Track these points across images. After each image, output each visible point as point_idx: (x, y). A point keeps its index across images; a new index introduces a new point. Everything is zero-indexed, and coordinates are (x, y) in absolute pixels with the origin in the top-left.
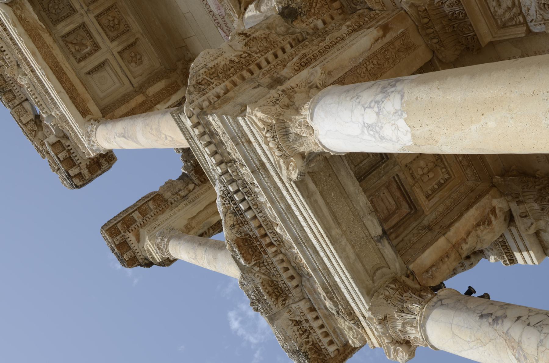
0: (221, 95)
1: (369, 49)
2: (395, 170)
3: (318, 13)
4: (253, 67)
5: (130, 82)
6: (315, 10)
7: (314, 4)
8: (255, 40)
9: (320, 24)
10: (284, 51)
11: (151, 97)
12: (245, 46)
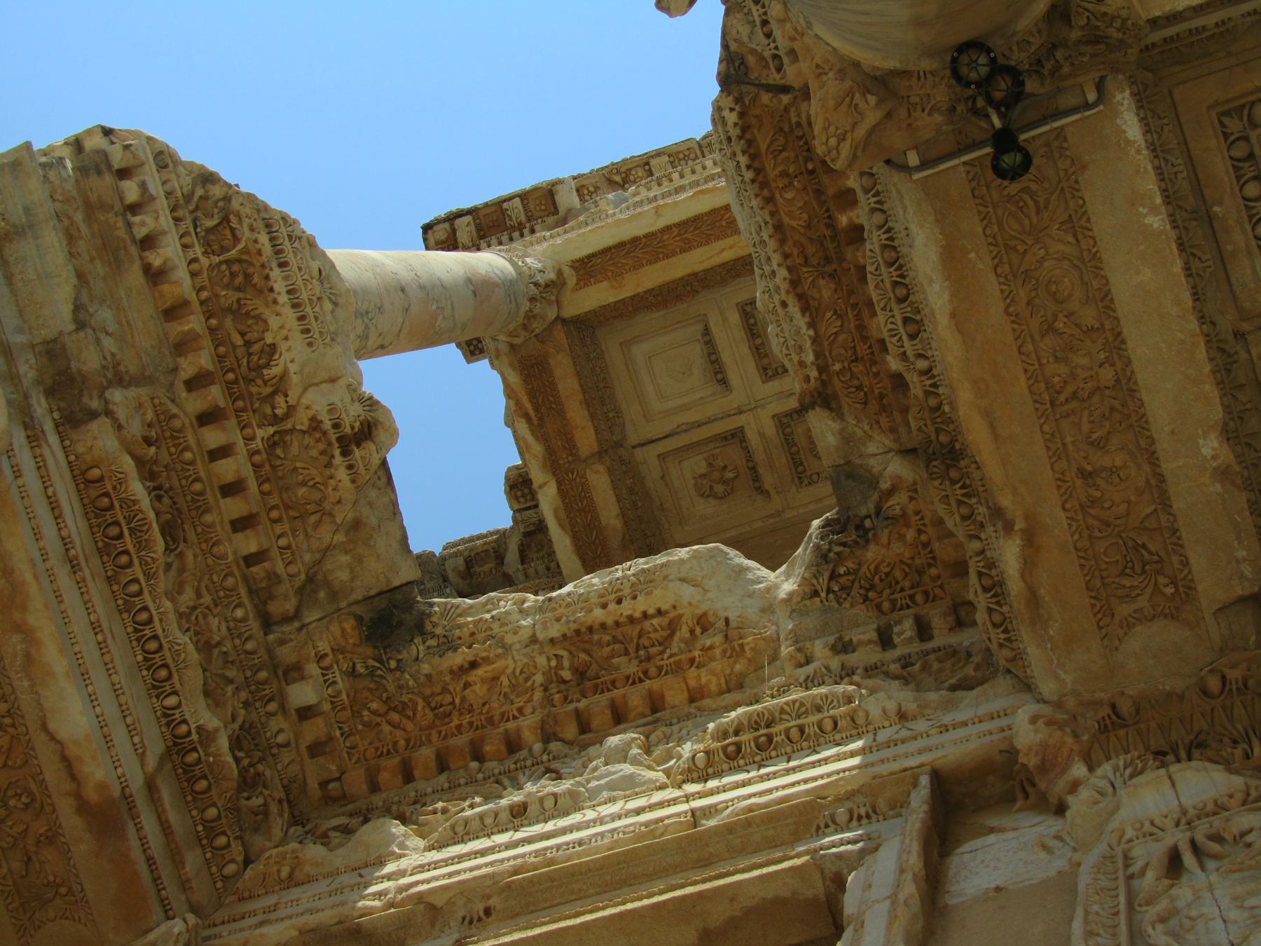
0: (147, 253)
1: (44, 727)
3: (356, 714)
4: (216, 394)
5: (652, 441)
6: (374, 713)
7: (395, 717)
8: (324, 459)
9: (303, 693)
10: (241, 524)
11: (583, 476)
12: (313, 419)
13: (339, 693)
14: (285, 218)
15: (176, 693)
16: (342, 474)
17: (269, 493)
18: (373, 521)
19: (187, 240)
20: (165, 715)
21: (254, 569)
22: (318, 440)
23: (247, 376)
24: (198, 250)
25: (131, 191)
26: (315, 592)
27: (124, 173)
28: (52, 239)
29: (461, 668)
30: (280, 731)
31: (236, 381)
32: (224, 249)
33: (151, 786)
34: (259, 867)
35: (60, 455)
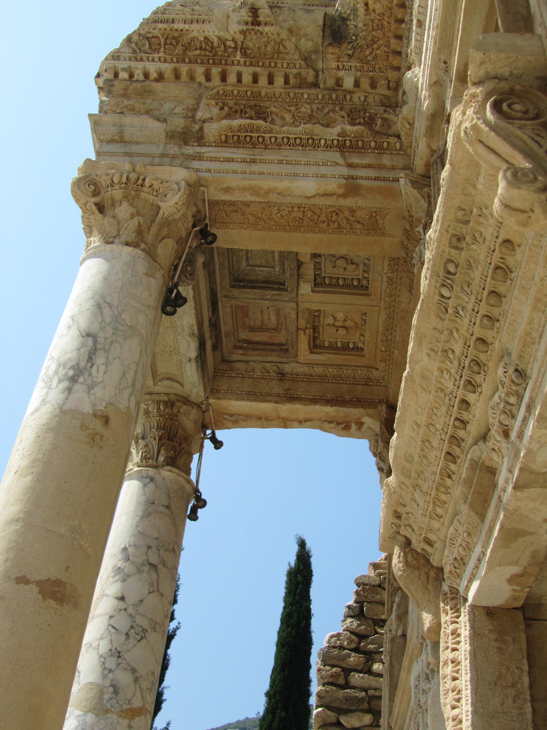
0: (151, 78)
1: (309, 198)
2: (288, 305)
3: (367, 62)
4: (215, 71)
6: (370, 54)
7: (375, 46)
8: (258, 34)
10: (271, 81)
12: (240, 33)
13: (356, 66)
14: (154, 13)
15: (320, 139)
16: (267, 29)
17: (264, 63)
18: (291, 23)
19: (150, 59)
20: (327, 147)
21: (291, 82)
22: (250, 34)
23: (213, 54)
24: (156, 56)
25: (123, 75)
26: (311, 59)
27: (116, 75)
28: (129, 119)
29: (366, 10)
30: (359, 98)
31: (214, 60)
32: (159, 44)
33: (350, 166)
34: (402, 134)
35: (211, 149)
